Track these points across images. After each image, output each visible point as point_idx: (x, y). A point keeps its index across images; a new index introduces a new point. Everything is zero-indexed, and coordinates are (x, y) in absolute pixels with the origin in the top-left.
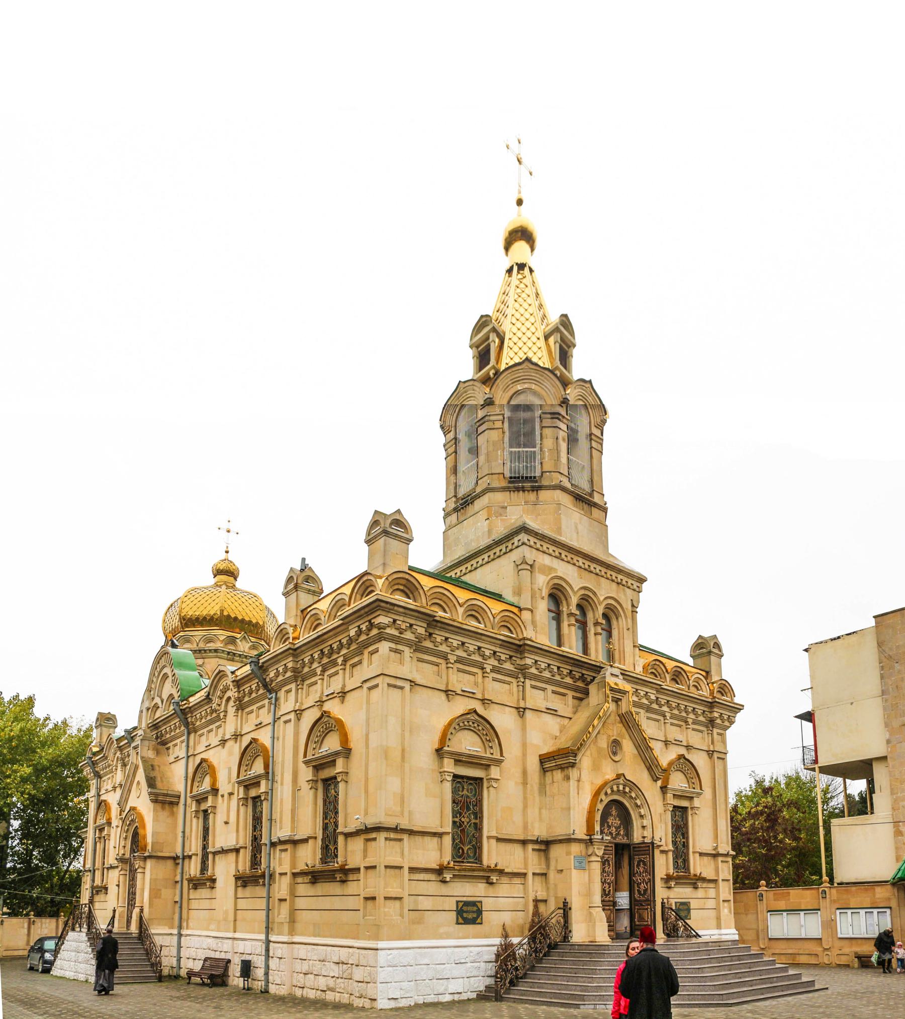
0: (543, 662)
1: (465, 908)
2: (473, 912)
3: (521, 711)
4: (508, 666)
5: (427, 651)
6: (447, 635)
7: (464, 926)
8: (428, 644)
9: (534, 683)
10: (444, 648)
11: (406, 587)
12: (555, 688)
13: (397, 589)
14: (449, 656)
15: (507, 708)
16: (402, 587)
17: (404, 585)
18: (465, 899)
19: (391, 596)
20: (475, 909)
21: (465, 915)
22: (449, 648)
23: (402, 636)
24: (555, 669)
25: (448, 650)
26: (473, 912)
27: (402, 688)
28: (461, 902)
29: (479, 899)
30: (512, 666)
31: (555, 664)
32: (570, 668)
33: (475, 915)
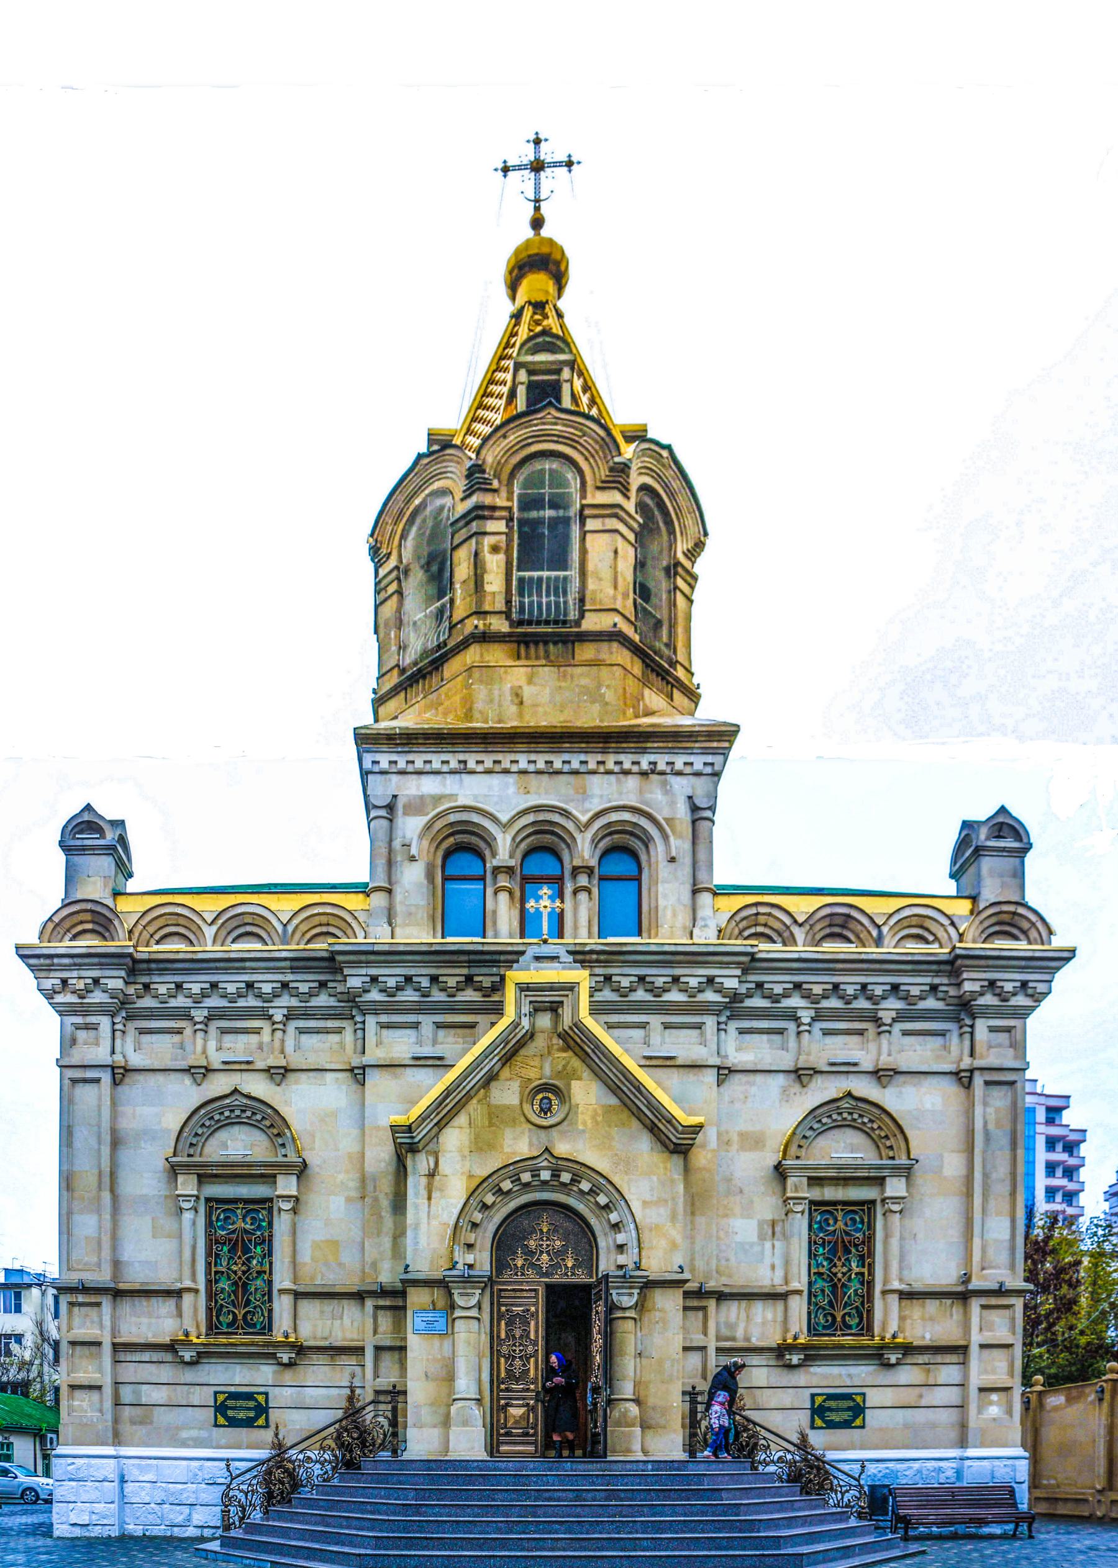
0: (391, 976)
1: (230, 1403)
2: (249, 1409)
3: (358, 1074)
4: (323, 1000)
5: (150, 1014)
6: (178, 979)
7: (230, 1429)
8: (148, 1002)
9: (384, 1018)
10: (180, 1001)
11: (97, 923)
12: (439, 1018)
13: (85, 931)
14: (193, 1013)
15: (329, 1075)
16: (89, 926)
17: (92, 922)
18: (232, 1389)
19: (73, 943)
20: (252, 1404)
21: (230, 1413)
22: (189, 1000)
23: (85, 1001)
24: (425, 983)
25: (188, 1003)
26: (249, 1409)
27: (97, 1081)
28: (224, 1393)
29: (262, 1389)
30: (332, 999)
31: (422, 974)
32: (465, 971)
33: (252, 1414)
